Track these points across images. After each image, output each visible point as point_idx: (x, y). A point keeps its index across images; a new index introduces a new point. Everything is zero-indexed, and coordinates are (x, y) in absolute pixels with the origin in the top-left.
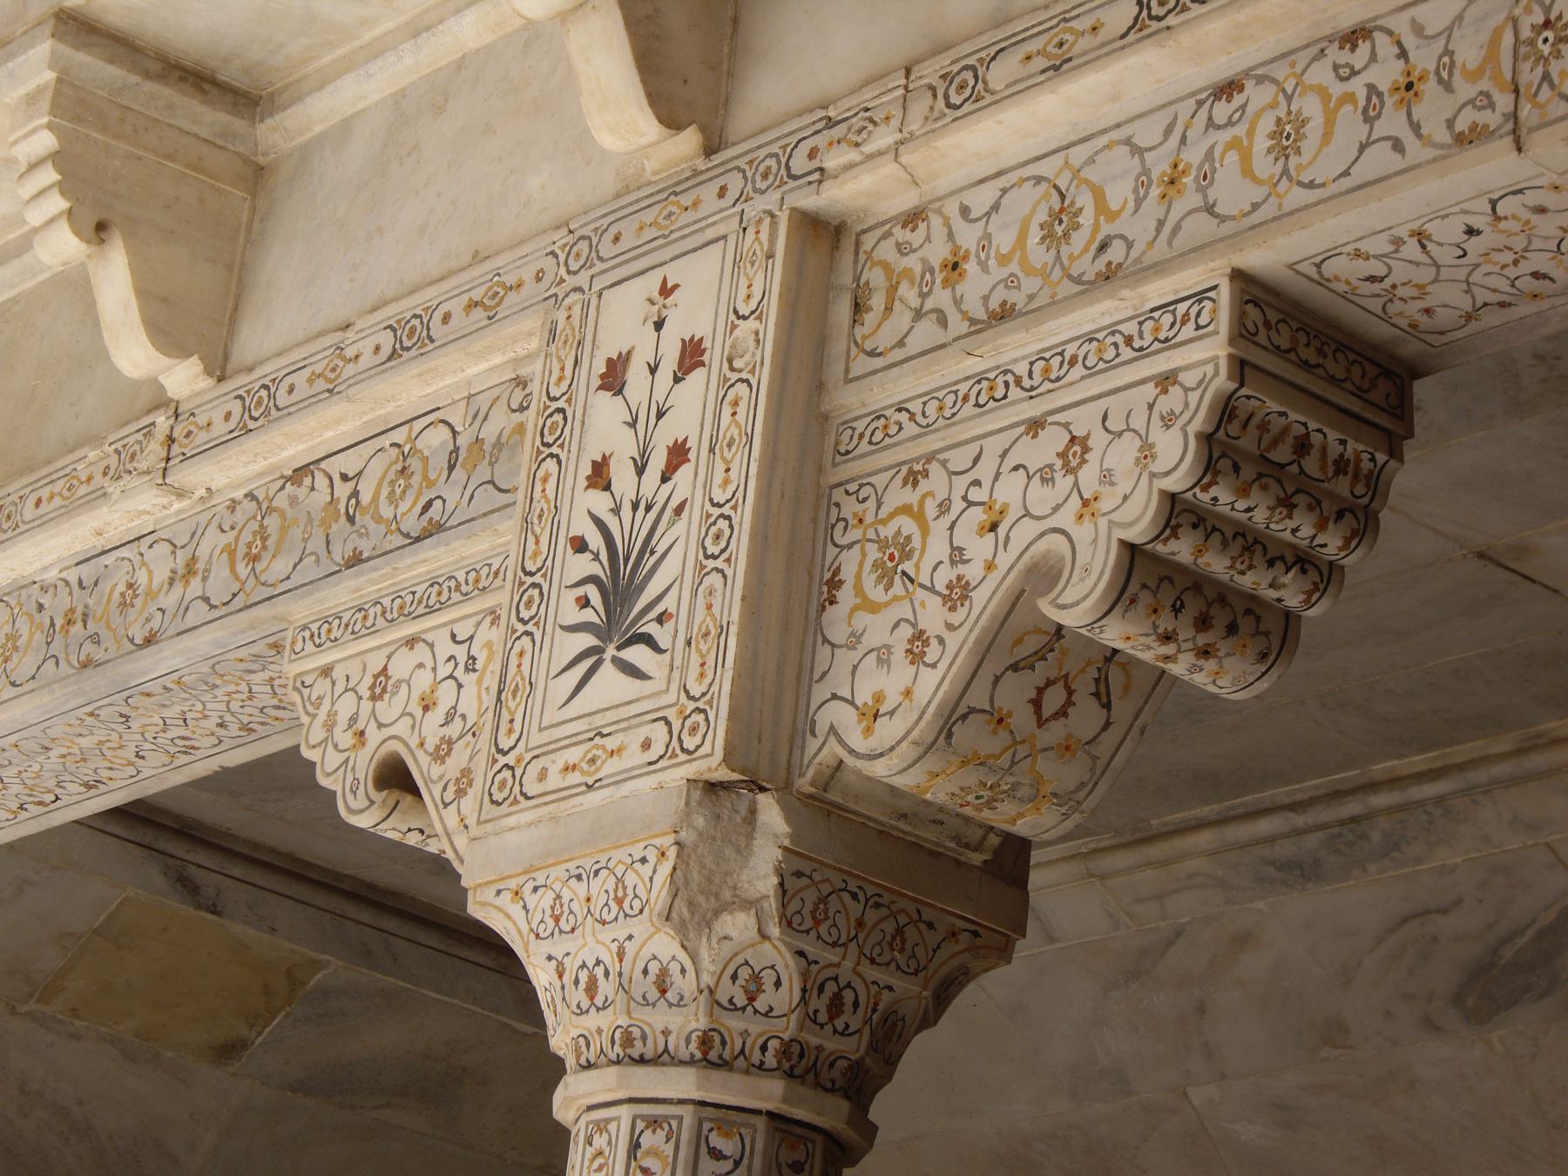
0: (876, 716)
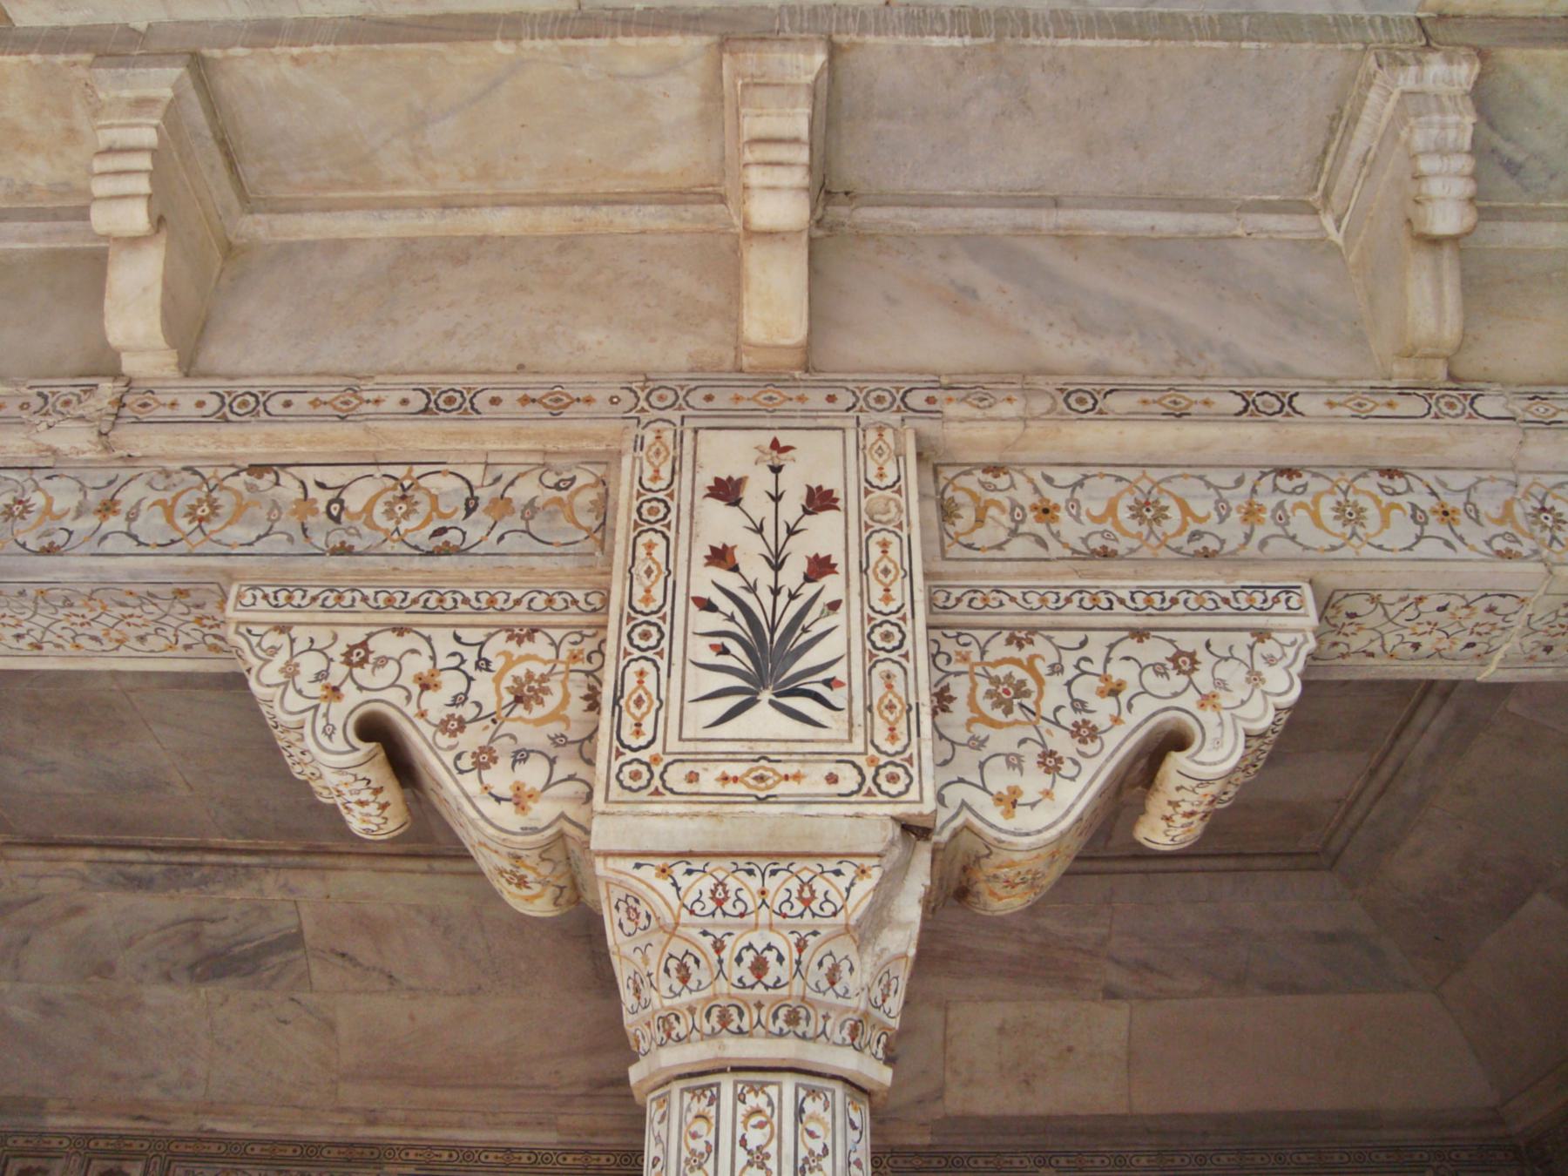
0: (1014, 804)
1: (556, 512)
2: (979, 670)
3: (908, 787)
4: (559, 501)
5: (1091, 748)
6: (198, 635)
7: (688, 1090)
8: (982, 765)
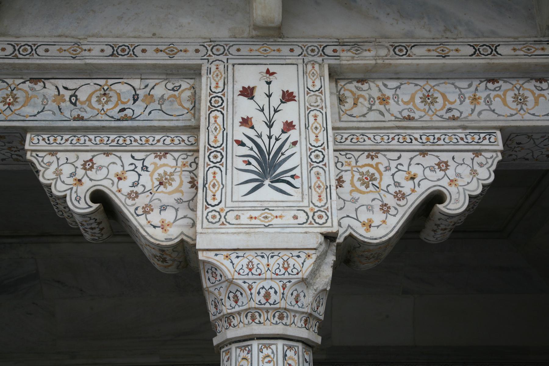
0: (370, 226)
1: (174, 101)
2: (355, 169)
3: (327, 220)
4: (174, 96)
5: (402, 202)
6: (9, 155)
7: (238, 347)
8: (356, 210)
